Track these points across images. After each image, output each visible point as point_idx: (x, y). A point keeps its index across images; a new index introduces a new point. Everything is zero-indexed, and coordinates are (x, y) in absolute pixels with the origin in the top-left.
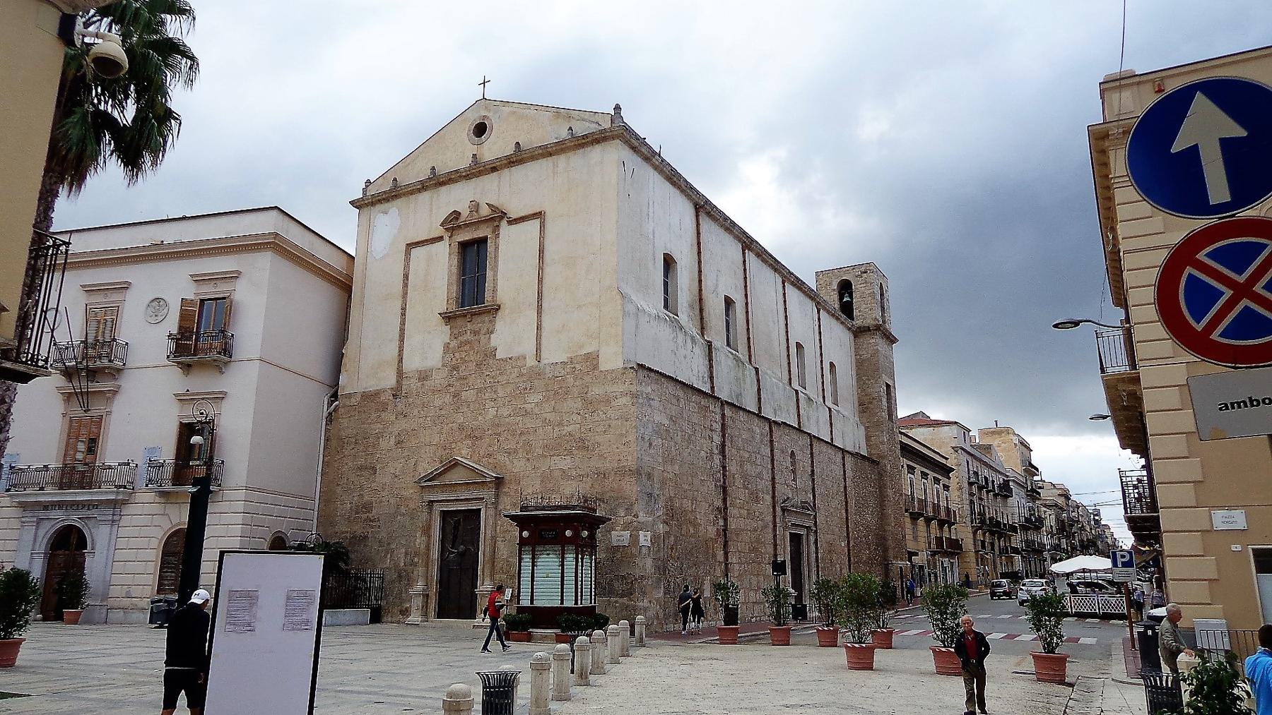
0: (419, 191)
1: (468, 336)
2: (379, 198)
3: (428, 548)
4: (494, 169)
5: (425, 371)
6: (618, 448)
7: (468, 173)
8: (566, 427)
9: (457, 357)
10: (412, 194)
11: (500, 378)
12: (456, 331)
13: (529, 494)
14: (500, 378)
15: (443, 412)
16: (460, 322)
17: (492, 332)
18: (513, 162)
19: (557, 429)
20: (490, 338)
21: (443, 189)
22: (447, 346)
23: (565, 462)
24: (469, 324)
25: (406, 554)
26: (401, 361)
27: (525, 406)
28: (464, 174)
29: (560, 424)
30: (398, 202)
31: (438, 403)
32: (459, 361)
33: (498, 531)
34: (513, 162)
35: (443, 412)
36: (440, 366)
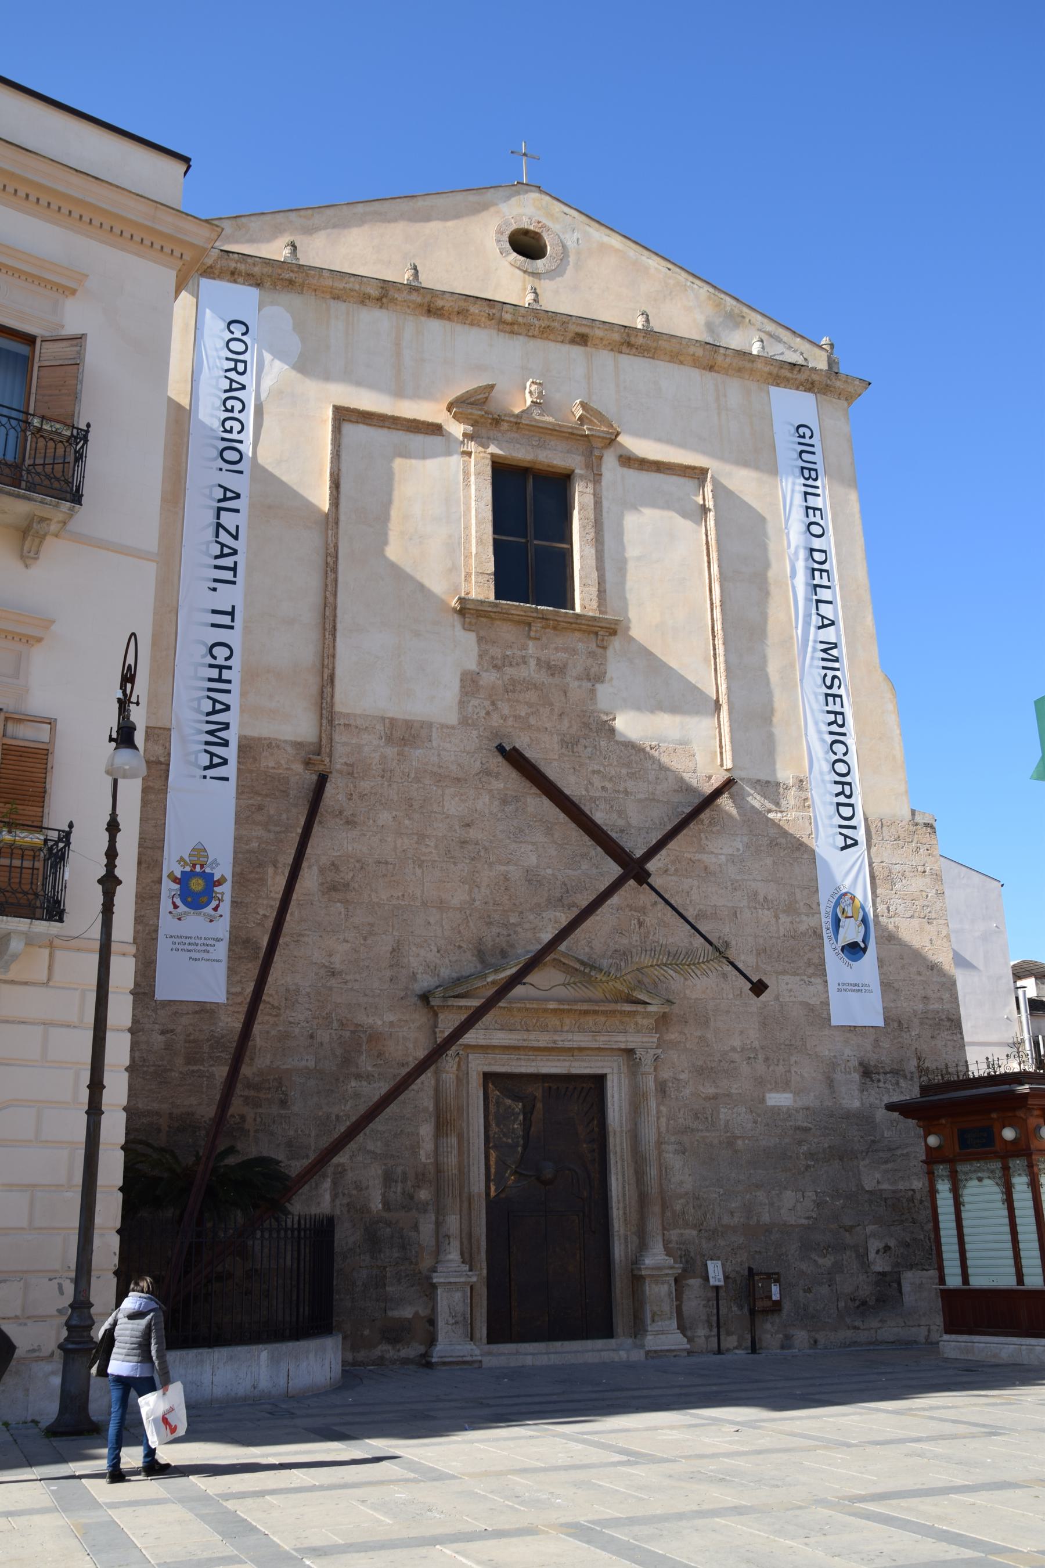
0: (364, 299)
1: (530, 671)
2: (242, 267)
3: (463, 1170)
4: (581, 339)
5: (409, 725)
6: (919, 974)
7: (520, 319)
8: (804, 918)
9: (506, 711)
10: (336, 298)
11: (630, 785)
12: (496, 651)
13: (733, 1049)
14: (630, 785)
15: (473, 833)
16: (507, 632)
17: (600, 678)
18: (630, 345)
19: (784, 918)
20: (593, 691)
21: (435, 326)
22: (469, 683)
23: (811, 988)
24: (531, 643)
25: (388, 1179)
26: (327, 680)
27: (705, 857)
28: (508, 317)
29: (791, 908)
30: (295, 300)
31: (453, 807)
32: (510, 722)
33: (663, 1129)
34: (630, 345)
35: (473, 833)
36: (453, 719)
